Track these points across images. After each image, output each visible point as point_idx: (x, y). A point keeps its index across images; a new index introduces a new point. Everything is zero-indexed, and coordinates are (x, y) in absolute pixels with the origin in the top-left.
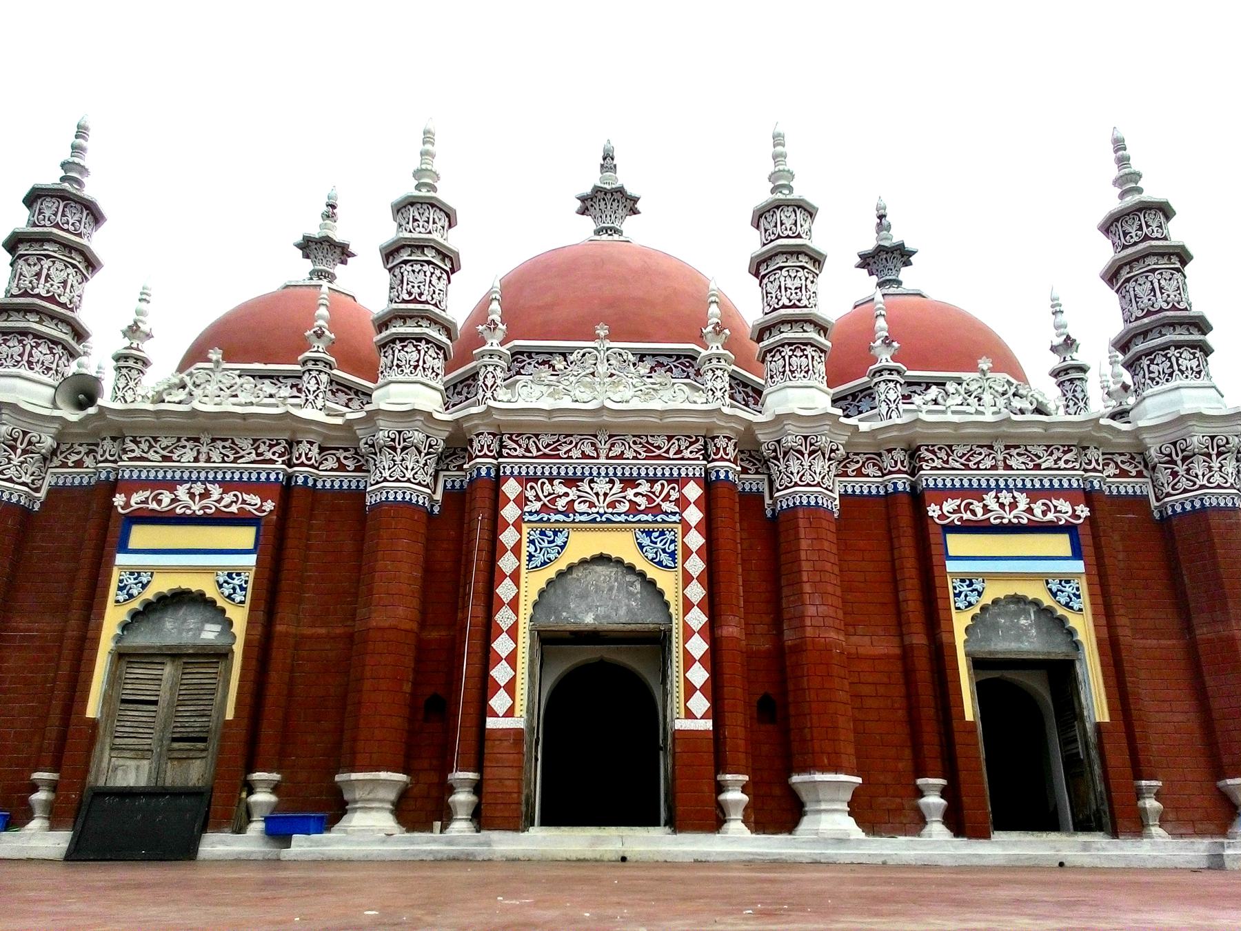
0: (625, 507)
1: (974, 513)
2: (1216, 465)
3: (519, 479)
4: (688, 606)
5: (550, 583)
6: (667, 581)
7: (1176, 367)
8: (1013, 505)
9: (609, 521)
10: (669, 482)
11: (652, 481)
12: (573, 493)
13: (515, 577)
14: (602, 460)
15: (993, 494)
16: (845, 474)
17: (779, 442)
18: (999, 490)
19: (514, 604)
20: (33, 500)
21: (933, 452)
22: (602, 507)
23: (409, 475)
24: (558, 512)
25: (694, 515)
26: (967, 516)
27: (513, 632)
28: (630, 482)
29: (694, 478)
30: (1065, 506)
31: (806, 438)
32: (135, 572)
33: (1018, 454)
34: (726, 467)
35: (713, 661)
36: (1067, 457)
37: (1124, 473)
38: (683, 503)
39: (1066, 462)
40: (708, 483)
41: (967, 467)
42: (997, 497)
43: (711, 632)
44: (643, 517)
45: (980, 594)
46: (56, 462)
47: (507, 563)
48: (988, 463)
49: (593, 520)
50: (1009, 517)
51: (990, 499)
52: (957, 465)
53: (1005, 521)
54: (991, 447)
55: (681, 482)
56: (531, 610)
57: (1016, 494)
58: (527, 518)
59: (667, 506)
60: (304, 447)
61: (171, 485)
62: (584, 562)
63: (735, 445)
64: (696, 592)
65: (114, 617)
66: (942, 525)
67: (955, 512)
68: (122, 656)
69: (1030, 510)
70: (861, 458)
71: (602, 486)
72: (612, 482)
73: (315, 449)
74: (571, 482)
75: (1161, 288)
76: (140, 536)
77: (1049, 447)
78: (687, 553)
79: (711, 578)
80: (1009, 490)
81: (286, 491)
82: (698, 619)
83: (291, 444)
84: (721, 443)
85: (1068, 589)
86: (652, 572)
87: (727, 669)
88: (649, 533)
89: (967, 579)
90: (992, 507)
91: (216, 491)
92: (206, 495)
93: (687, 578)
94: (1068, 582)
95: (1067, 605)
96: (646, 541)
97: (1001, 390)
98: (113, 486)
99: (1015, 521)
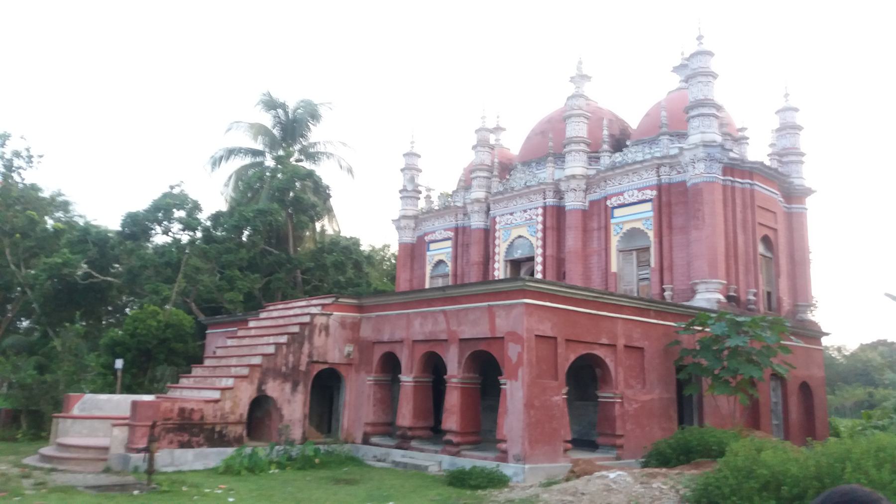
0: (524, 219)
1: (620, 200)
2: (696, 166)
3: (499, 216)
4: (538, 247)
5: (509, 245)
6: (533, 240)
7: (701, 123)
8: (633, 195)
9: (520, 225)
10: (535, 208)
11: (530, 209)
12: (511, 217)
13: (499, 246)
14: (518, 206)
15: (626, 192)
16: (591, 194)
17: (569, 186)
18: (628, 191)
19: (499, 254)
20: (414, 240)
21: (611, 181)
22: (519, 221)
23: (476, 220)
24: (507, 224)
25: (540, 219)
26: (619, 202)
27: (499, 262)
28: (525, 211)
29: (541, 207)
30: (648, 192)
31: (578, 185)
32: (430, 256)
33: (637, 175)
34: (550, 201)
35: (544, 264)
36: (652, 173)
37: (679, 173)
38: (537, 215)
39: (652, 175)
40: (545, 208)
41: (620, 184)
42: (628, 193)
43: (544, 255)
44: (528, 222)
45: (621, 229)
46: (417, 229)
47: (497, 242)
48: (627, 180)
49: (515, 225)
50: (631, 200)
51: (626, 195)
52: (617, 184)
53: (629, 202)
54: (628, 175)
55: (537, 208)
56: (504, 254)
57: (634, 191)
58: (501, 227)
59: (534, 217)
60: (459, 215)
61: (434, 232)
62: (516, 238)
63: (555, 192)
64: (540, 243)
65: (428, 269)
66: (612, 207)
67: (616, 201)
68: (432, 278)
69: (637, 197)
70: (595, 187)
71: (519, 214)
72: (521, 212)
73: (462, 216)
74: (511, 214)
75: (701, 90)
76: (433, 246)
77: (646, 170)
78: (538, 230)
79: (544, 239)
80: (631, 190)
81: (456, 230)
82: (540, 251)
83: (457, 215)
84: (547, 193)
85: (649, 223)
86: (531, 238)
87: (547, 266)
88: (529, 227)
89: (617, 224)
90: (627, 198)
91: (443, 231)
92: (441, 233)
93: (538, 239)
94: (648, 220)
95: (647, 228)
96: (529, 229)
97: (634, 150)
98: (426, 234)
99: (632, 201)
